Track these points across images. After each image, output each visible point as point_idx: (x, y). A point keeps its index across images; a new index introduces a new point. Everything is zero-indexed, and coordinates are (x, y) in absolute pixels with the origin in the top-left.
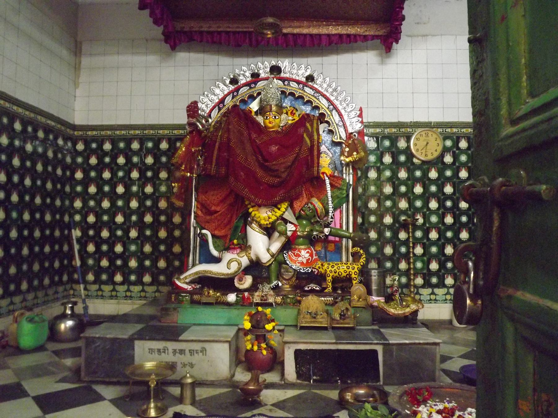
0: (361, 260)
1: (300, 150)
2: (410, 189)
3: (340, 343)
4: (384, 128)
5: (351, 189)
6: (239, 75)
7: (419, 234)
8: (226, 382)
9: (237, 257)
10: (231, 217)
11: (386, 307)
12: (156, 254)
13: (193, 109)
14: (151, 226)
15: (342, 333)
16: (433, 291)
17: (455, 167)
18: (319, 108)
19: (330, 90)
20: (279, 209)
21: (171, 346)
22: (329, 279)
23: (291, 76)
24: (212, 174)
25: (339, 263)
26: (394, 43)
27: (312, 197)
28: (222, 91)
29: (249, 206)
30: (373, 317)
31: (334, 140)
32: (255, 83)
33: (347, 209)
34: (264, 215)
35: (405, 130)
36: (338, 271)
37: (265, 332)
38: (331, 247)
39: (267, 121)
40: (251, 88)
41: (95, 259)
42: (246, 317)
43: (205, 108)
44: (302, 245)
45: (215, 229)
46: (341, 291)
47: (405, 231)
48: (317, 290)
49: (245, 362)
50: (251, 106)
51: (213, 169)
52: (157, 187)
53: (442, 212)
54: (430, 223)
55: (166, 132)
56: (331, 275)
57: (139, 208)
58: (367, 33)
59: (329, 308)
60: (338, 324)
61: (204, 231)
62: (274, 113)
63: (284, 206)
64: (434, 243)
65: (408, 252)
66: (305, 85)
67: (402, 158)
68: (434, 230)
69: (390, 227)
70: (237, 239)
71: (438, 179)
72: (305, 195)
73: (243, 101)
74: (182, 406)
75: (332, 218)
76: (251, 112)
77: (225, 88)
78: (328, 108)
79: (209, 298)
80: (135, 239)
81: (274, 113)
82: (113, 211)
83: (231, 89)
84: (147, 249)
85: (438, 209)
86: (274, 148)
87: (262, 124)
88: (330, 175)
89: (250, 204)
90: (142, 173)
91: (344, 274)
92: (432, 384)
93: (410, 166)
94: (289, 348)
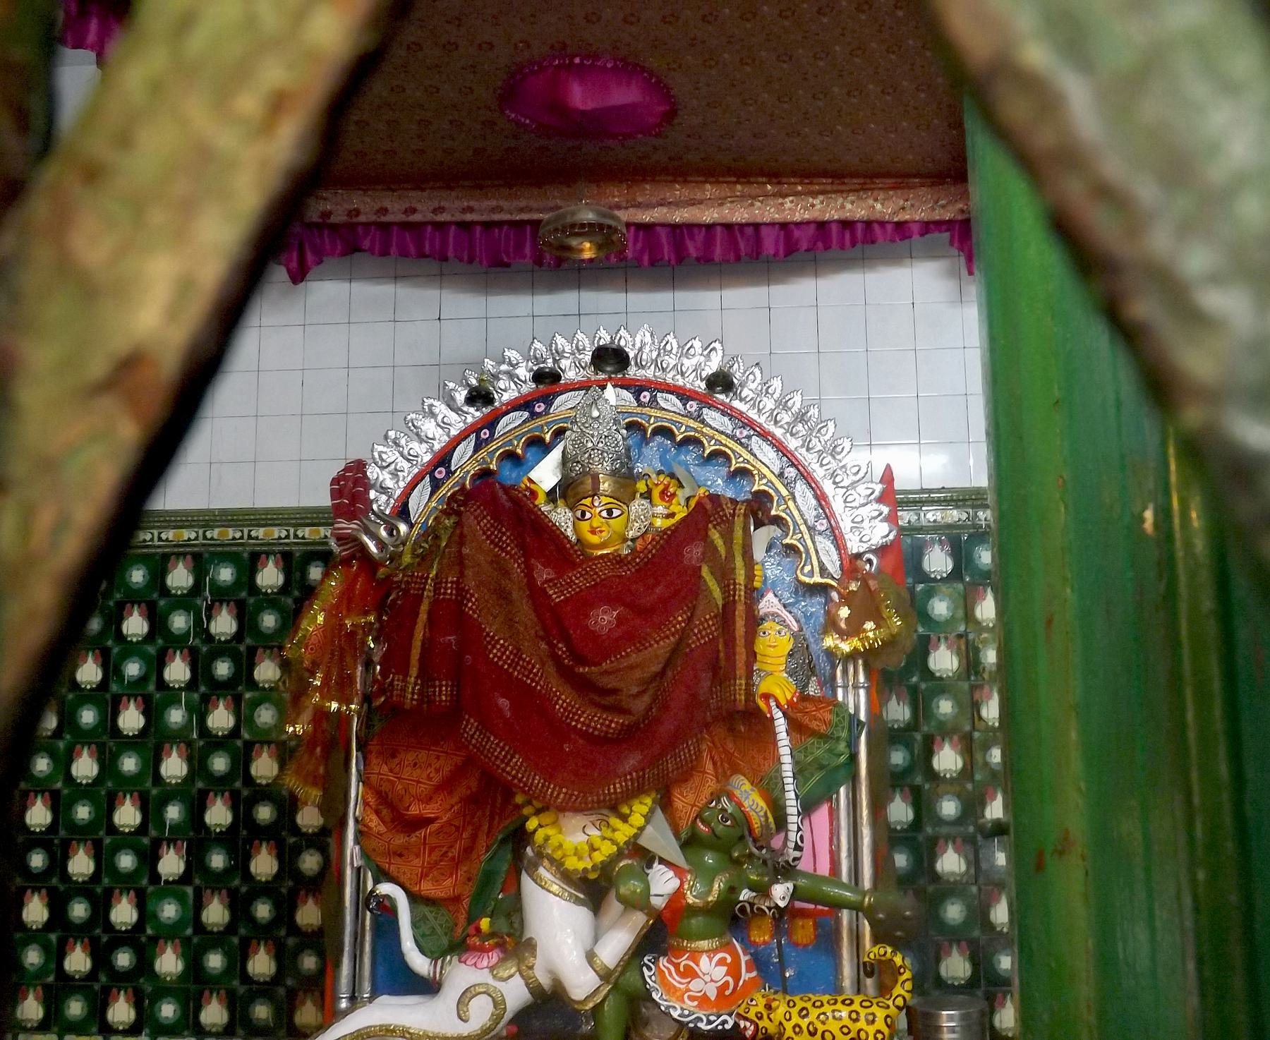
0: (898, 990)
1: (690, 619)
4: (973, 507)
5: (863, 738)
6: (496, 377)
10: (474, 838)
12: (242, 931)
13: (351, 487)
14: (228, 839)
18: (753, 476)
19: (786, 418)
20: (625, 818)
24: (407, 707)
25: (825, 998)
28: (444, 425)
29: (527, 811)
32: (548, 399)
33: (850, 807)
34: (577, 838)
36: (821, 1028)
38: (804, 931)
39: (585, 526)
40: (534, 415)
41: (46, 948)
43: (389, 483)
45: (423, 876)
50: (533, 475)
51: (410, 687)
55: (277, 532)
57: (189, 779)
58: (906, 217)
61: (386, 888)
62: (605, 500)
63: (640, 808)
66: (705, 401)
72: (709, 767)
73: (510, 456)
75: (798, 848)
76: (534, 494)
77: (453, 417)
78: (781, 475)
80: (174, 882)
81: (605, 500)
82: (105, 793)
83: (470, 420)
84: (216, 913)
86: (605, 618)
87: (569, 533)
88: (790, 703)
89: (529, 803)
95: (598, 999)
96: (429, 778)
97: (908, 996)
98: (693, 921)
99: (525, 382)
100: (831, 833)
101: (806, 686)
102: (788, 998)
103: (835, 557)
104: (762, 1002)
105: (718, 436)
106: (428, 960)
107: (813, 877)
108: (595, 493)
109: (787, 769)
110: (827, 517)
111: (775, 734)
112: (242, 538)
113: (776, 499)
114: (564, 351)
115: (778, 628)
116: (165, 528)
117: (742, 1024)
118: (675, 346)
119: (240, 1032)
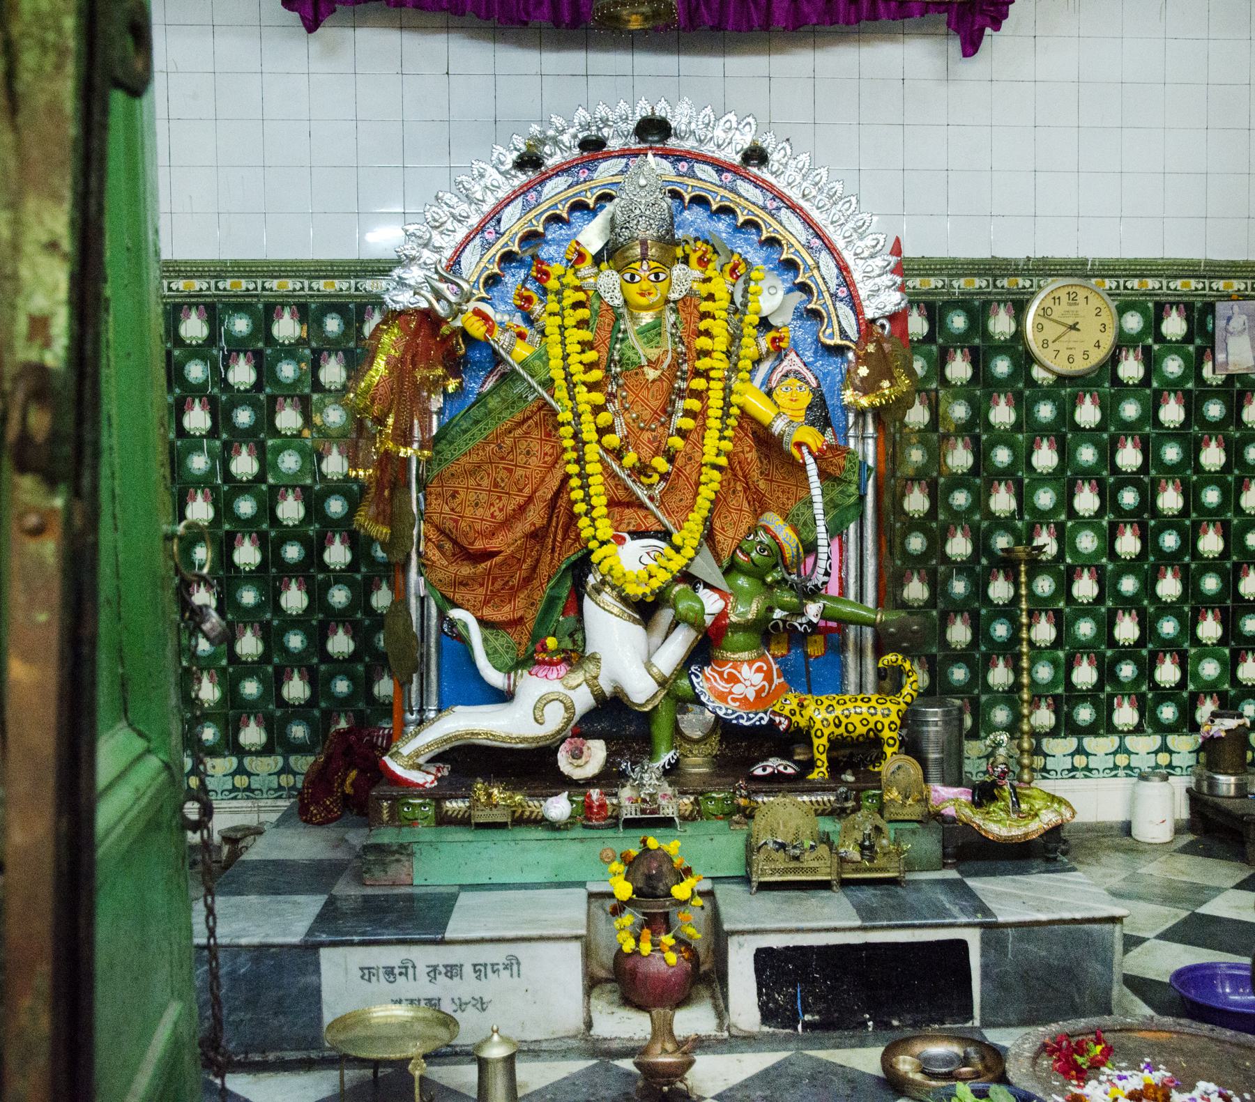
2: (1024, 457)
3: (874, 928)
4: (949, 276)
5: (871, 482)
7: (1045, 585)
8: (574, 1043)
11: (977, 819)
15: (867, 894)
17: (1148, 391)
18: (780, 245)
22: (820, 743)
23: (696, 144)
25: (847, 697)
26: (988, 31)
30: (944, 848)
37: (672, 905)
39: (633, 289)
42: (617, 867)
44: (744, 650)
45: (486, 602)
46: (854, 775)
47: (1007, 578)
48: (789, 775)
49: (607, 981)
52: (269, 457)
53: (1111, 520)
54: (1075, 552)
55: (290, 284)
56: (827, 732)
59: (827, 825)
60: (856, 871)
61: (455, 614)
64: (1086, 611)
65: (1015, 639)
67: (1002, 367)
69: (964, 568)
70: (554, 635)
71: (1102, 427)
79: (495, 811)
81: (653, 264)
83: (516, 183)
85: (1100, 513)
88: (820, 450)
90: (221, 416)
91: (863, 730)
92: (1106, 1020)
93: (1023, 391)
94: (741, 946)
95: (656, 702)
96: (493, 516)
98: (736, 637)
99: (570, 148)
100: (841, 561)
101: (823, 434)
103: (854, 322)
104: (796, 701)
105: (752, 208)
106: (502, 675)
107: (832, 599)
108: (644, 257)
109: (818, 507)
110: (847, 285)
111: (807, 478)
112: (256, 289)
115: (799, 383)
116: (177, 277)
117: (777, 719)
119: (278, 749)
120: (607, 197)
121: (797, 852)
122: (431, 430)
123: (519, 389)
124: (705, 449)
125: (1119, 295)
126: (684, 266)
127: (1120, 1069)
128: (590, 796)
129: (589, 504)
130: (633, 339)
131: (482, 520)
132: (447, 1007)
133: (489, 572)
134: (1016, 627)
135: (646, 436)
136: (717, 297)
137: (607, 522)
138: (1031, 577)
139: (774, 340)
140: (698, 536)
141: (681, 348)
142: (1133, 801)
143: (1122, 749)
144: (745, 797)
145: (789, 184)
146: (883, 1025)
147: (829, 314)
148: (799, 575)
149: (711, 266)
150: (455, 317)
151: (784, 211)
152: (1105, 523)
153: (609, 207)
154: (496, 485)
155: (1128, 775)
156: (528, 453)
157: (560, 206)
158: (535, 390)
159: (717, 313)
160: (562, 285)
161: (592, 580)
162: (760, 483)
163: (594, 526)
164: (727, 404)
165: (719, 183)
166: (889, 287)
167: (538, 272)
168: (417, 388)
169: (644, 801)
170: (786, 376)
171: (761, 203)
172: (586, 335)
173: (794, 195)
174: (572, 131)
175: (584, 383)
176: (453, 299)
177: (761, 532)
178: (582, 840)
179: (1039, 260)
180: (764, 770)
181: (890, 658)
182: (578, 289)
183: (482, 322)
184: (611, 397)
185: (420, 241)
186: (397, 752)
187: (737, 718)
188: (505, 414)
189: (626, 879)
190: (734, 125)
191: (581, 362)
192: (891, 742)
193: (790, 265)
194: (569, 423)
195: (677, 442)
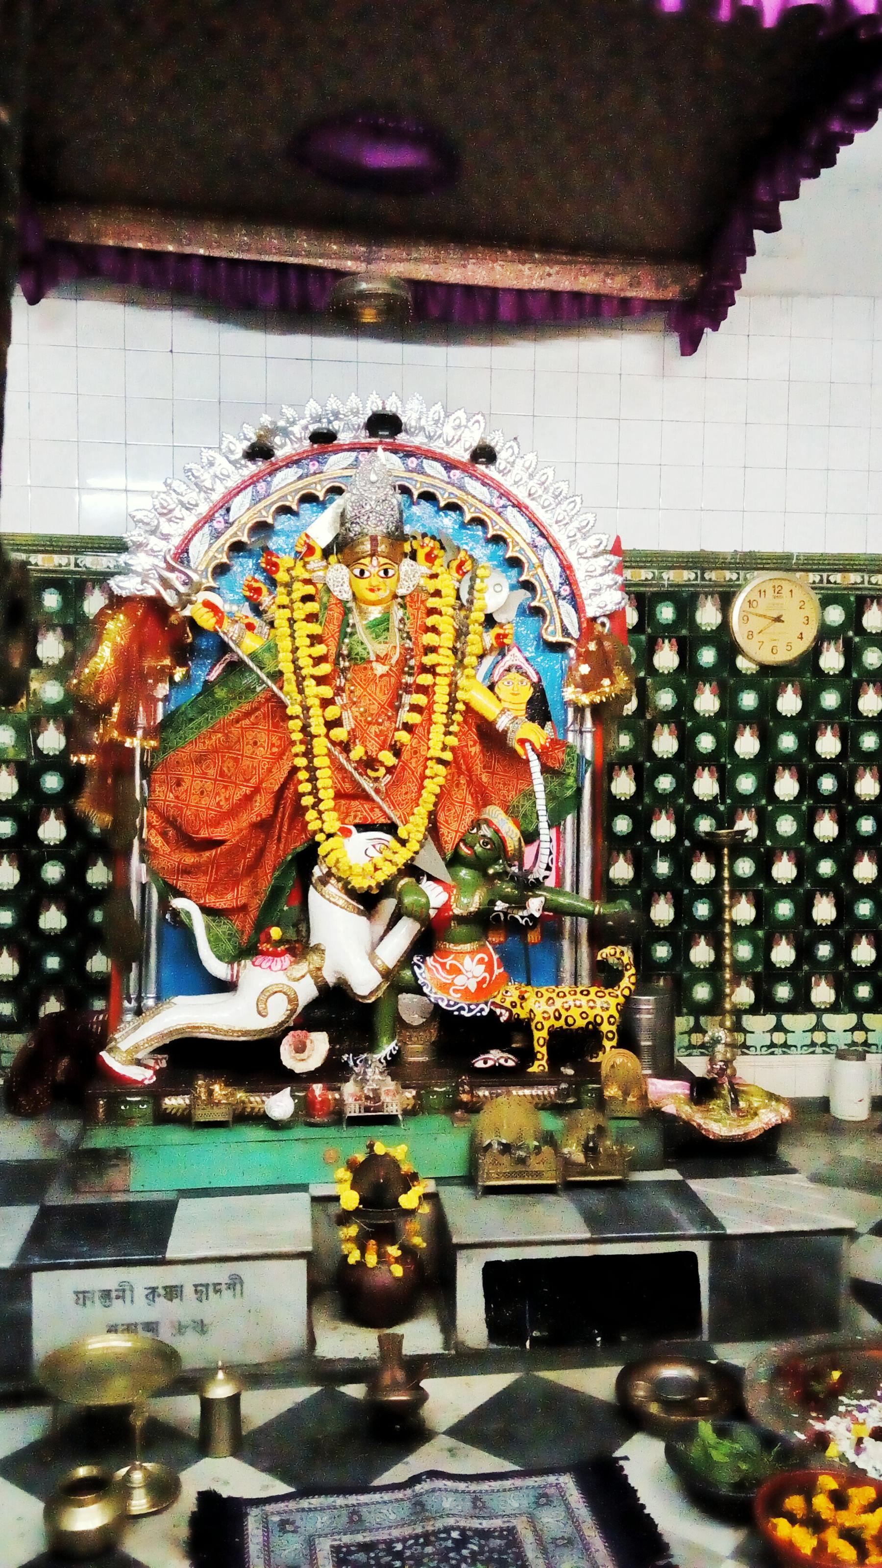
2: (726, 743)
4: (659, 568)
5: (588, 776)
7: (745, 867)
9: (285, 981)
11: (697, 1117)
16: (779, 1021)
17: (848, 681)
21: (142, 1277)
22: (540, 1036)
23: (426, 440)
27: (487, 803)
31: (545, 637)
35: (717, 575)
36: (564, 1014)
39: (363, 584)
44: (465, 942)
45: (209, 890)
56: (547, 1024)
59: (551, 1123)
61: (178, 903)
67: (707, 656)
68: (785, 857)
69: (669, 849)
70: (278, 925)
74: (206, 1462)
79: (216, 1110)
81: (383, 560)
85: (799, 799)
88: (543, 747)
91: (581, 1023)
93: (728, 680)
94: (470, 1260)
95: (380, 994)
97: (633, 987)
99: (300, 440)
102: (536, 990)
103: (575, 620)
104: (517, 993)
107: (549, 890)
113: (526, 565)
114: (338, 413)
117: (498, 1011)
118: (442, 414)
120: (337, 491)
121: (522, 1153)
122: (155, 719)
123: (247, 681)
124: (431, 743)
125: (822, 588)
126: (412, 562)
127: (859, 1397)
128: (313, 1091)
129: (316, 797)
130: (362, 634)
131: (208, 809)
132: (166, 1335)
133: (212, 862)
134: (718, 910)
135: (374, 729)
136: (443, 593)
137: (335, 815)
138: (733, 859)
139: (498, 636)
140: (423, 829)
141: (409, 644)
142: (831, 1079)
143: (819, 1027)
144: (468, 1093)
145: (516, 483)
146: (611, 1340)
147: (551, 612)
148: (521, 867)
149: (436, 563)
150: (184, 607)
151: (510, 509)
152: (804, 808)
153: (339, 501)
154: (222, 774)
155: (825, 1052)
156: (255, 743)
157: (290, 498)
158: (263, 682)
159: (444, 610)
160: (292, 578)
161: (317, 872)
162: (483, 776)
163: (320, 818)
164: (453, 700)
165: (447, 479)
166: (610, 587)
167: (267, 564)
168: (142, 677)
169: (367, 1098)
170: (508, 670)
171: (488, 501)
172: (315, 629)
173: (521, 494)
174: (303, 422)
175: (313, 677)
176: (183, 589)
177: (484, 827)
178: (305, 1140)
179: (745, 554)
180: (485, 1063)
181: (606, 952)
182: (307, 582)
183: (212, 614)
184: (339, 691)
185: (148, 528)
186: (115, 1047)
187: (459, 1009)
188: (233, 705)
189: (353, 1187)
190: (464, 422)
191: (310, 656)
192: (610, 1035)
193: (515, 563)
194: (297, 717)
195: (403, 737)
